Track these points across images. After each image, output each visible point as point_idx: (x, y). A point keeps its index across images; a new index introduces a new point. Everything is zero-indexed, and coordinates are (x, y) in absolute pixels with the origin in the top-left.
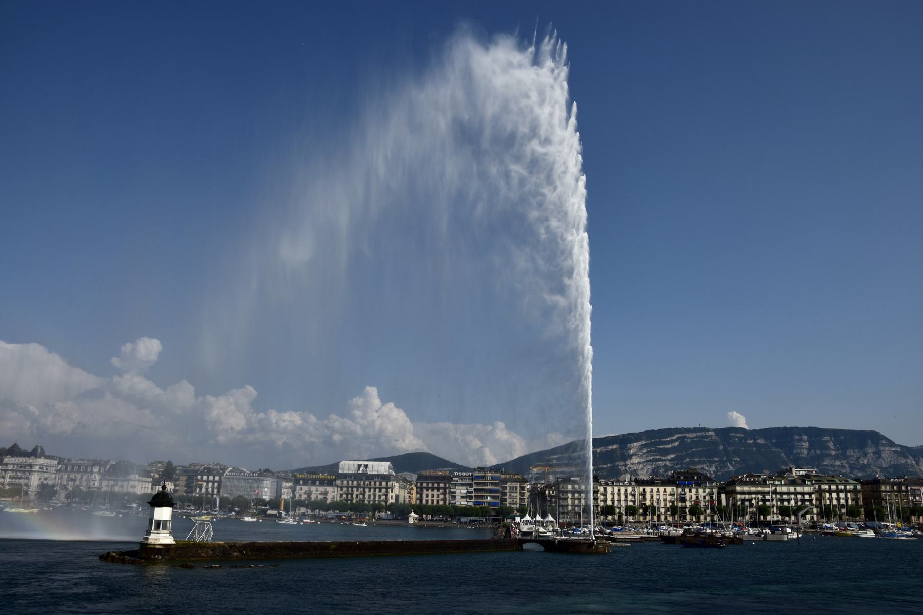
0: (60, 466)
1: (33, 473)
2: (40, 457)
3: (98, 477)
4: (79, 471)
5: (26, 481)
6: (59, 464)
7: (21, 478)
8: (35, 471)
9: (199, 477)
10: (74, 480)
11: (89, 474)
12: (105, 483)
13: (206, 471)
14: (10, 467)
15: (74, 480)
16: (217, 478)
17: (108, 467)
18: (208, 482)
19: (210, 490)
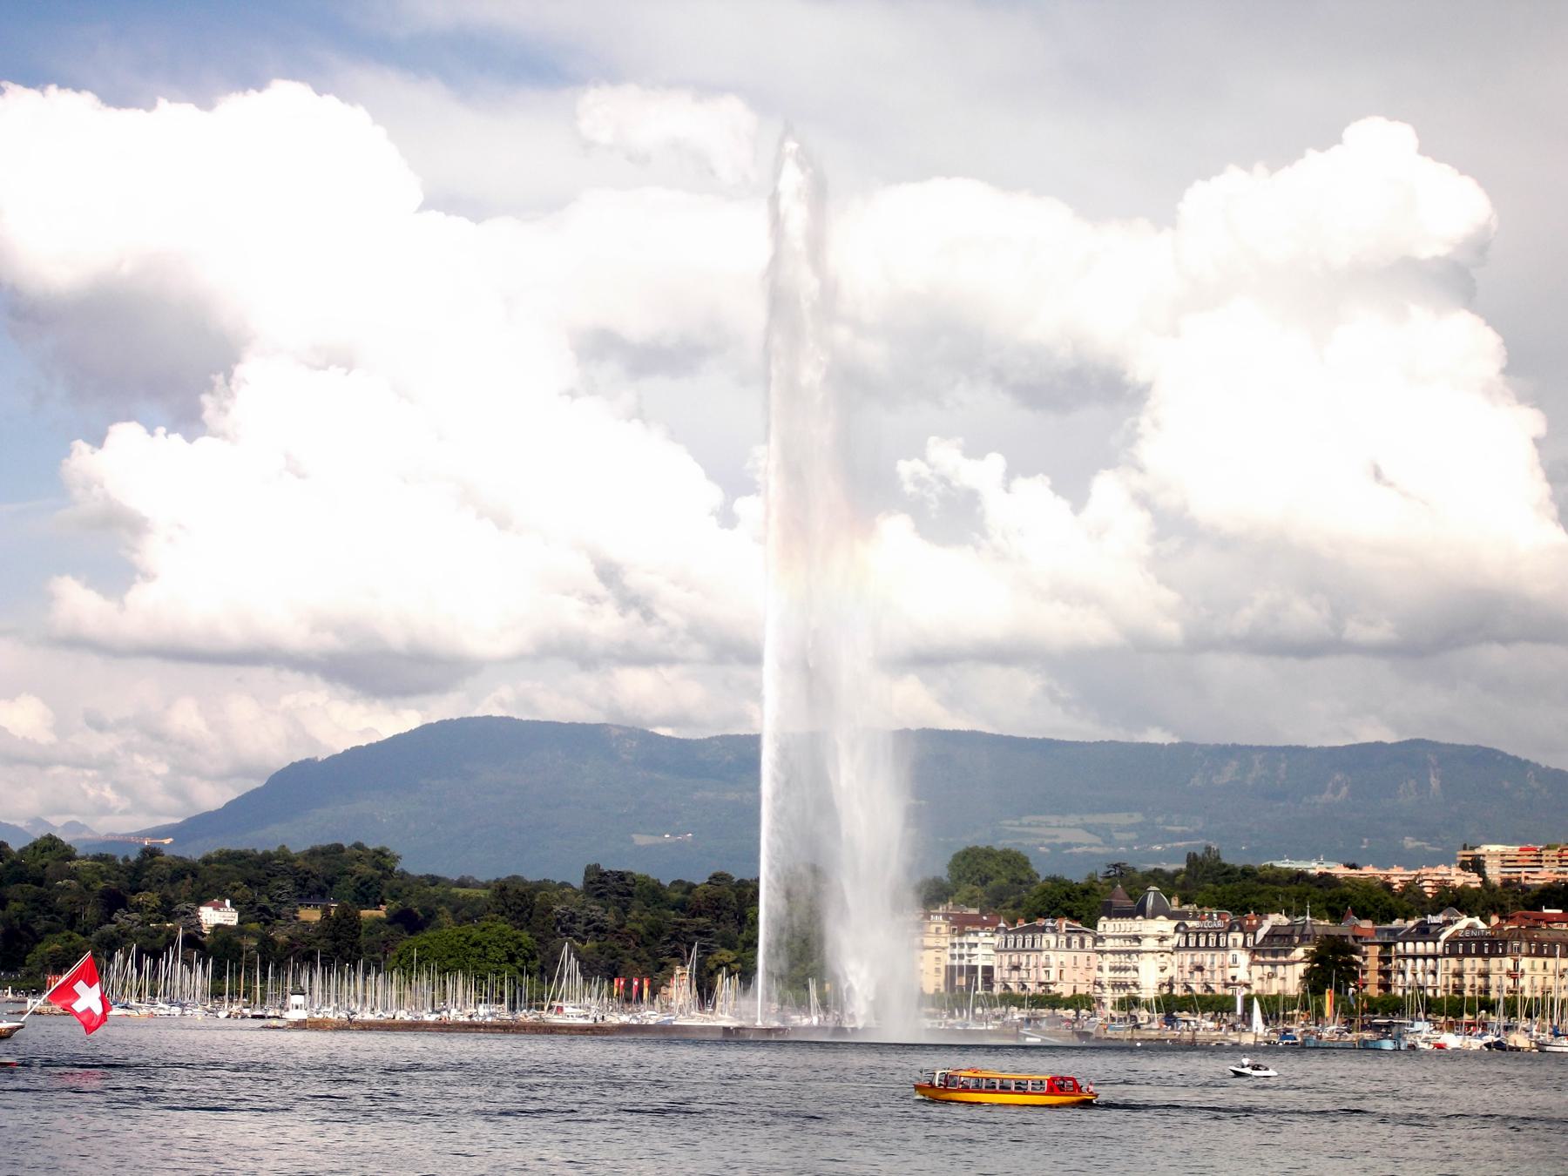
0: (1178, 935)
1: (1144, 954)
2: (1153, 917)
3: (1244, 958)
4: (1207, 947)
5: (1132, 974)
6: (1177, 930)
7: (1126, 969)
8: (1146, 952)
9: (1400, 945)
10: (1200, 969)
11: (1224, 953)
12: (1257, 971)
13: (1415, 930)
14: (1109, 944)
15: (1200, 969)
16: (1430, 945)
17: (1261, 933)
18: (1415, 958)
19: (1420, 976)
